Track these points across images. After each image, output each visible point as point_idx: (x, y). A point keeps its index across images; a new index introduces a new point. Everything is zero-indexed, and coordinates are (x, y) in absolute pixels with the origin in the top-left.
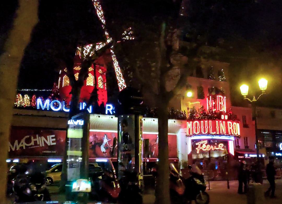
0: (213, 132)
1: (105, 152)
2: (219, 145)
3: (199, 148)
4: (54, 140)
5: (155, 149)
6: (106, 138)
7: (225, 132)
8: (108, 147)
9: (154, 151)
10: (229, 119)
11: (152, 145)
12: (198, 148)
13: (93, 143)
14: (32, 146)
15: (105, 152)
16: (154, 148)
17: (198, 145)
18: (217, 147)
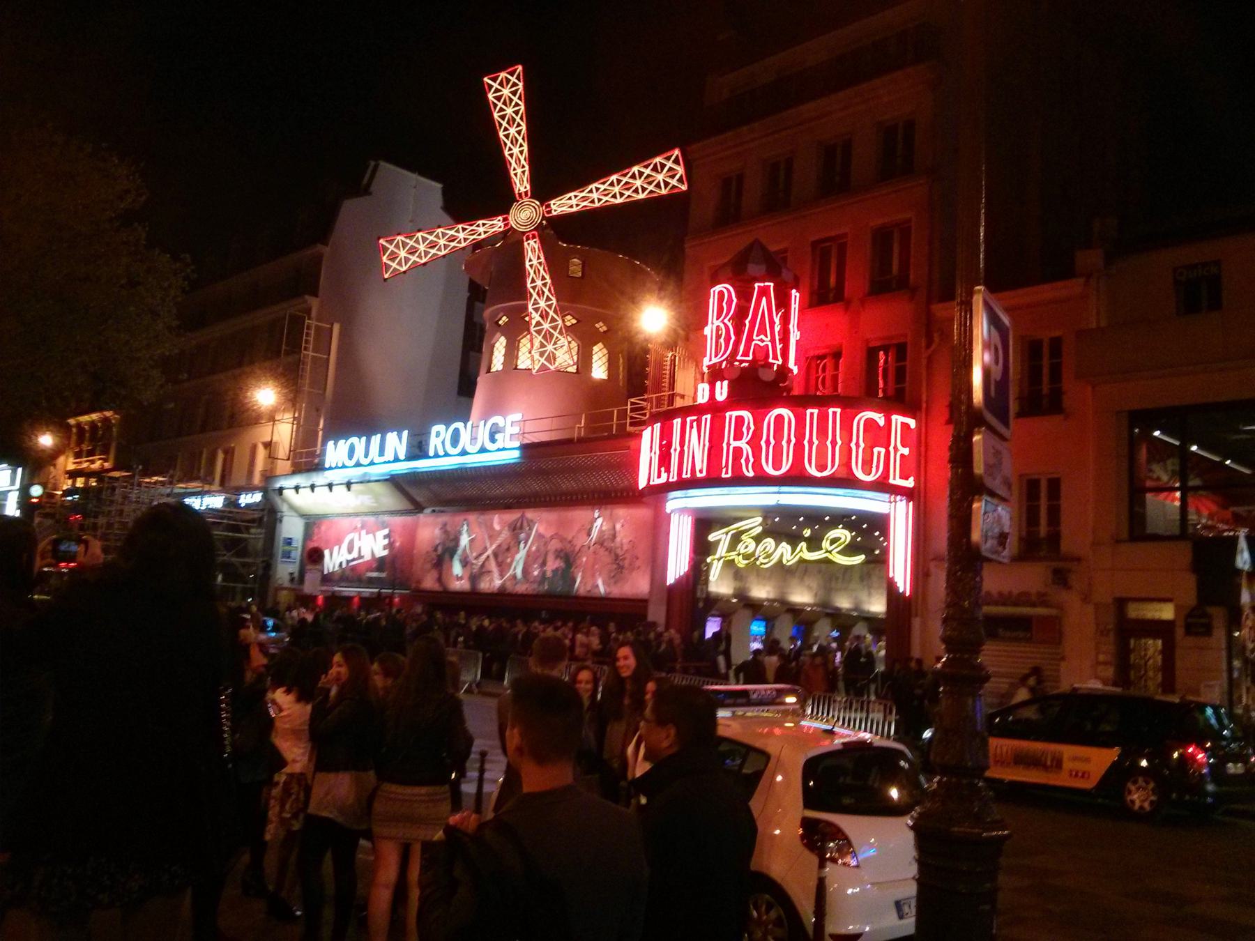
0: (659, 476)
1: (459, 576)
2: (825, 544)
3: (722, 558)
4: (386, 541)
5: (586, 561)
6: (467, 530)
7: (701, 471)
8: (468, 560)
9: (580, 574)
10: (735, 401)
11: (577, 549)
12: (717, 556)
13: (440, 549)
14: (354, 560)
15: (459, 576)
16: (582, 561)
17: (718, 542)
18: (814, 544)
